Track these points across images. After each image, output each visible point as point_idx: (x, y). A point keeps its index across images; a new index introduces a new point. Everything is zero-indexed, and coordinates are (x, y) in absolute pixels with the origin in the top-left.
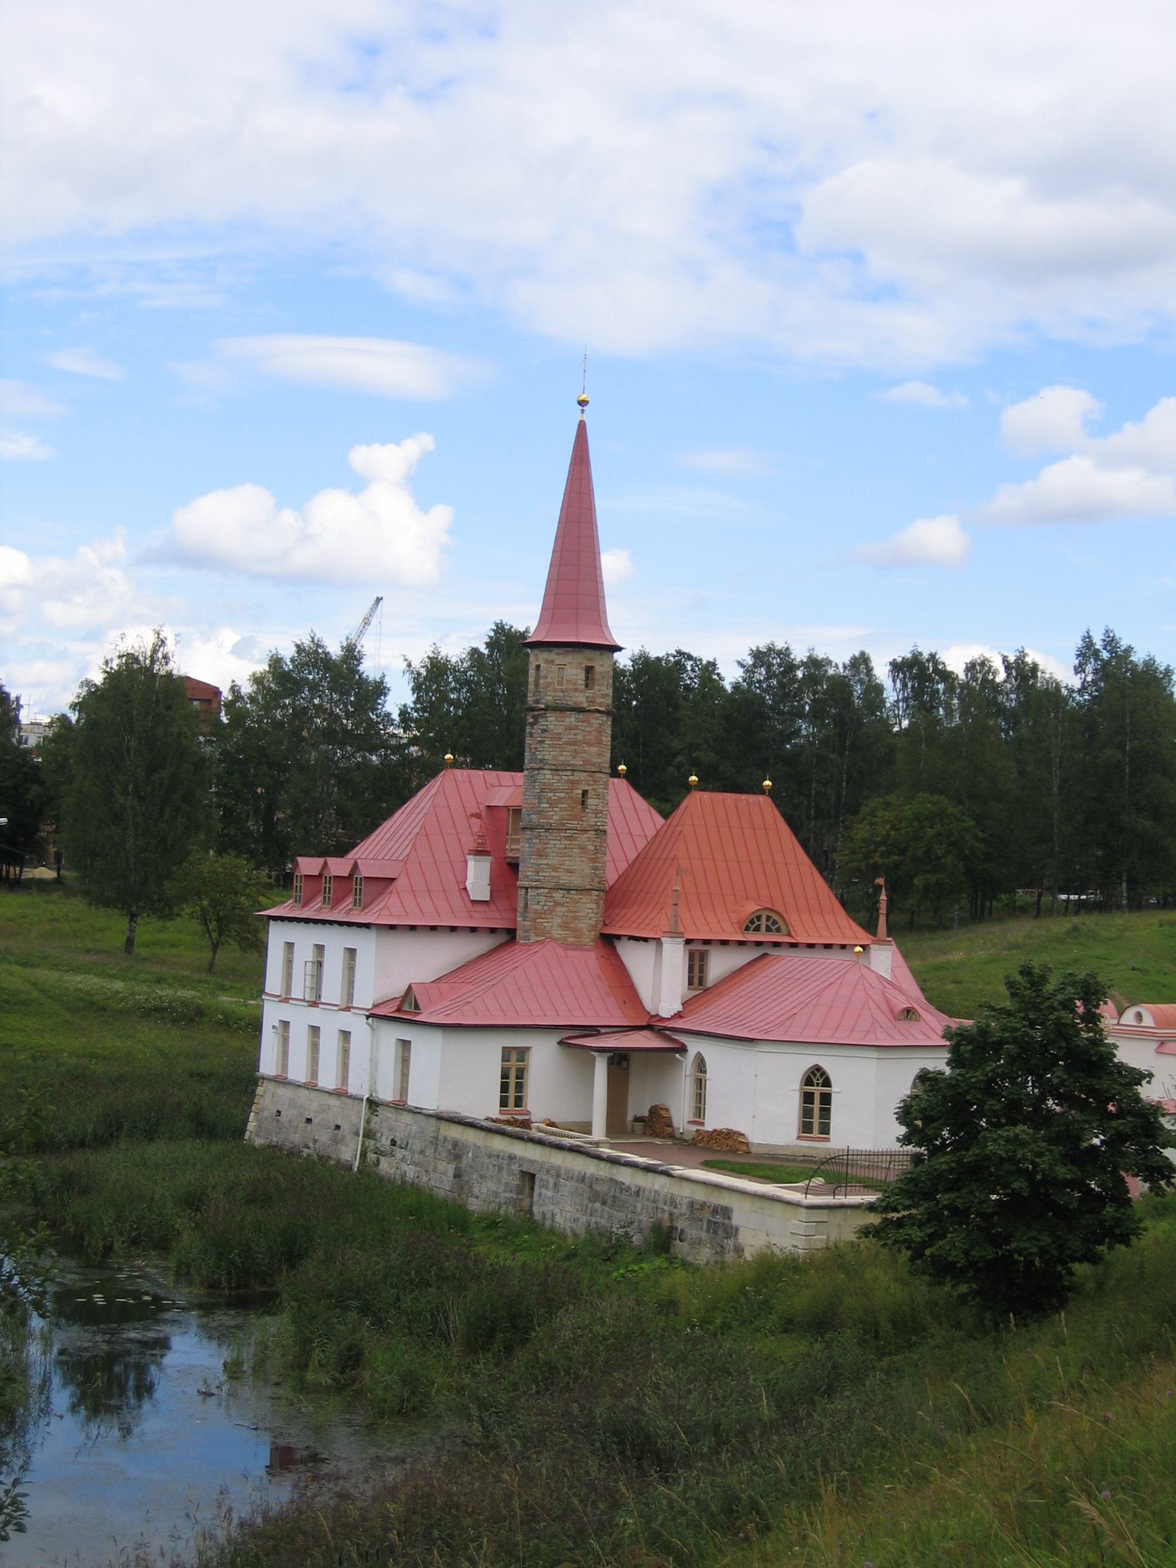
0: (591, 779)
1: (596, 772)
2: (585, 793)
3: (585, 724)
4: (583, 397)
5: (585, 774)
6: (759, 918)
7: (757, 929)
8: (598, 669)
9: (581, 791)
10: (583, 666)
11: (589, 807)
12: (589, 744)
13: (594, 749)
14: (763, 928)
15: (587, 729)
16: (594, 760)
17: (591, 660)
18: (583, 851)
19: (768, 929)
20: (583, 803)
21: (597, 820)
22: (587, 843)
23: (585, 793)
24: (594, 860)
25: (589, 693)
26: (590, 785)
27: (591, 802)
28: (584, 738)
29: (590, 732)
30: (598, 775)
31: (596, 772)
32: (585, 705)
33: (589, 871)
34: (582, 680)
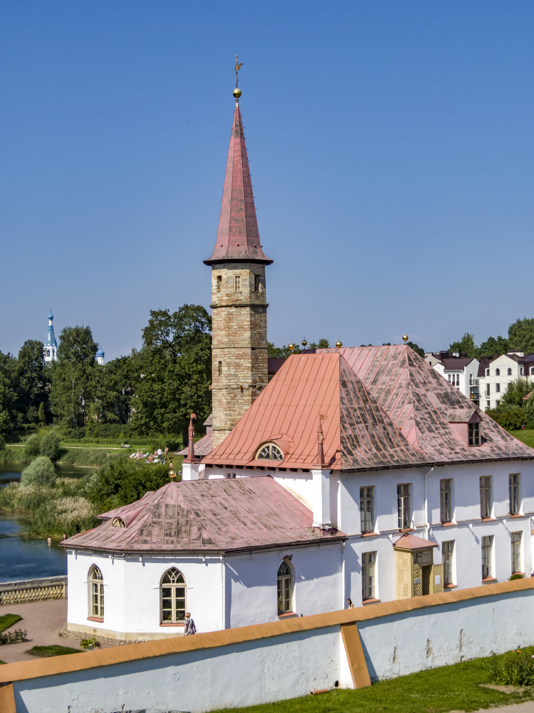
0: (222, 353)
1: (225, 348)
2: (220, 362)
3: (218, 316)
4: (236, 91)
5: (219, 350)
6: (268, 447)
7: (268, 457)
8: (224, 277)
9: (217, 363)
10: (216, 276)
11: (223, 373)
12: (221, 330)
13: (223, 332)
14: (270, 454)
15: (220, 319)
16: (224, 340)
17: (220, 272)
18: (220, 403)
19: (275, 457)
20: (220, 370)
21: (227, 381)
22: (222, 398)
23: (220, 362)
24: (225, 410)
25: (219, 295)
26: (222, 357)
27: (224, 369)
28: (218, 326)
29: (221, 321)
30: (226, 350)
31: (225, 348)
32: (217, 303)
33: (223, 417)
34: (215, 286)
